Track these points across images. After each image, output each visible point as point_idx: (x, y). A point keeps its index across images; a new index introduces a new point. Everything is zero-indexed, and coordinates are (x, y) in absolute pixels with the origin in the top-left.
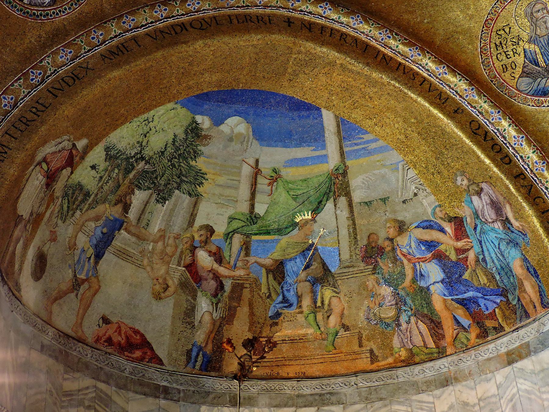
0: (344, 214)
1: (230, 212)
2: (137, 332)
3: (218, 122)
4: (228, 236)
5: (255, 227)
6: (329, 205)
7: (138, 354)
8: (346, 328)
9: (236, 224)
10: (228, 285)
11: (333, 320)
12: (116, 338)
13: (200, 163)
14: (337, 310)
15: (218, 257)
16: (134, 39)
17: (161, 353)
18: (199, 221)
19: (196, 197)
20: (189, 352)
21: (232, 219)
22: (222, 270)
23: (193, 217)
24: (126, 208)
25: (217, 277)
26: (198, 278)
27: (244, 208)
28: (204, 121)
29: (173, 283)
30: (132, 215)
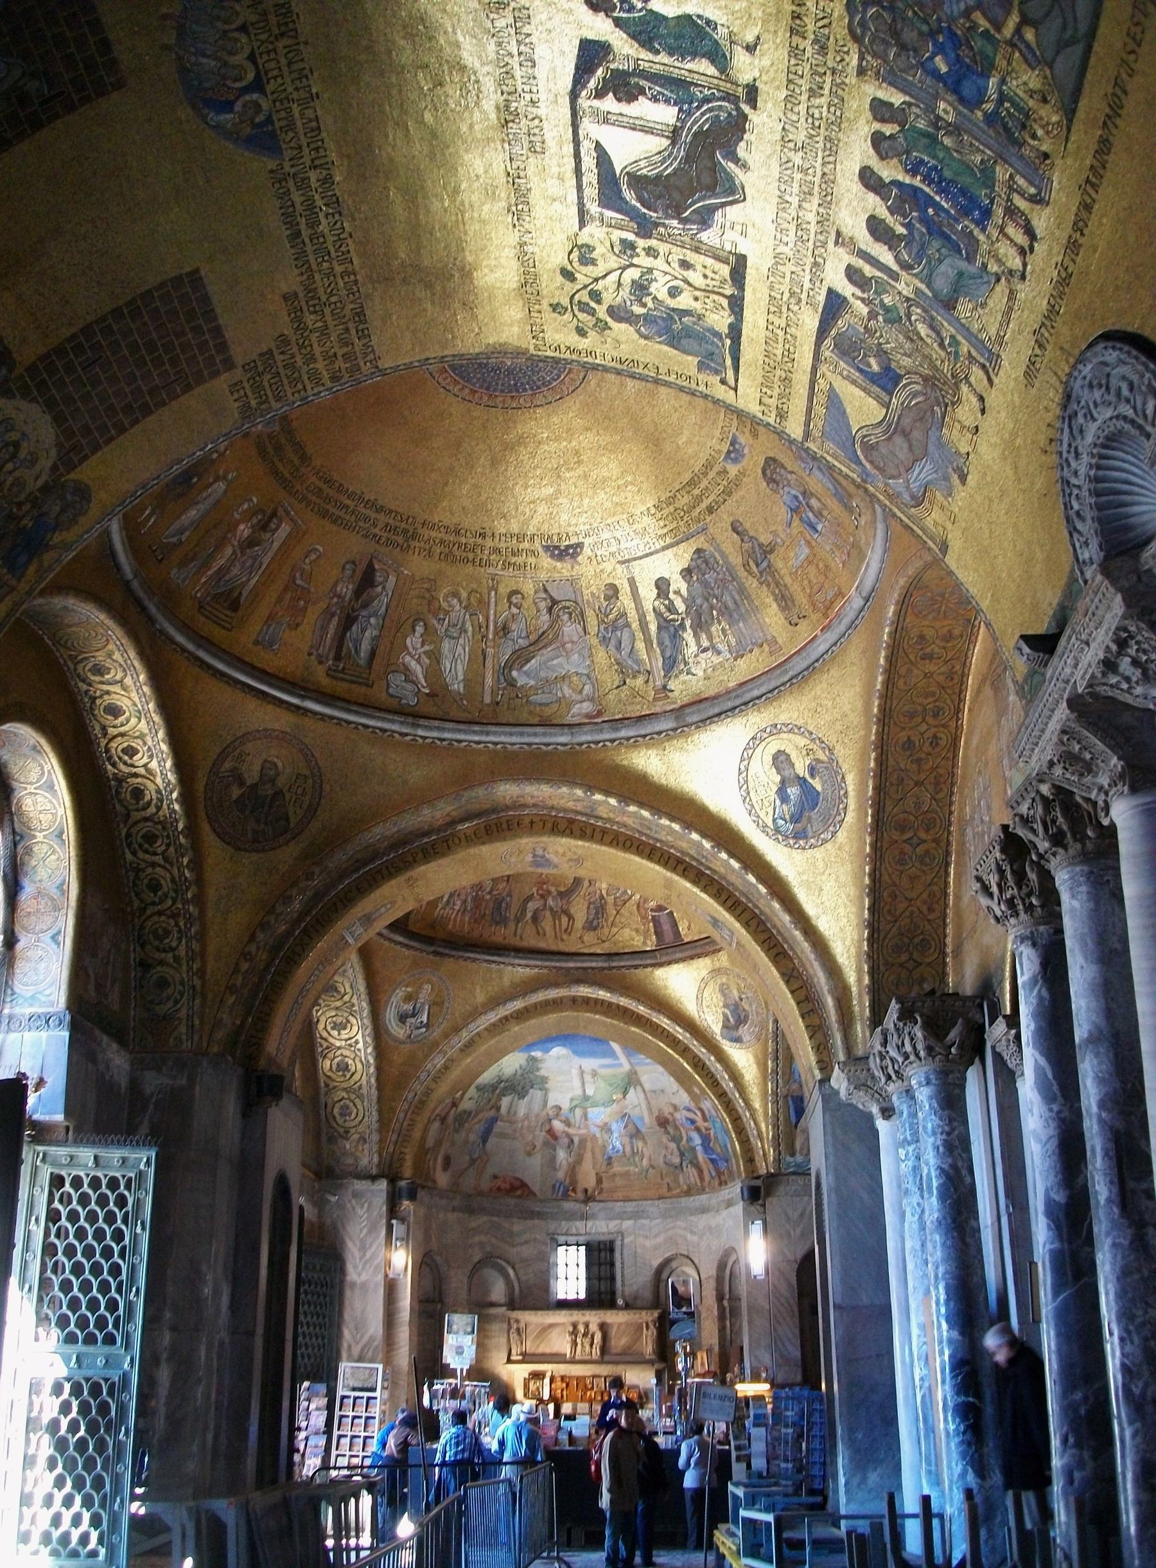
0: (642, 1096)
1: (570, 1096)
2: (517, 1179)
3: (548, 1051)
4: (572, 1109)
5: (588, 1104)
6: (632, 1090)
7: (519, 1192)
8: (653, 1167)
9: (575, 1103)
10: (576, 1140)
11: (645, 1162)
12: (503, 1186)
13: (543, 1073)
14: (646, 1154)
15: (568, 1123)
16: (478, 1034)
17: (535, 1189)
18: (551, 1103)
19: (546, 1091)
20: (554, 1186)
21: (572, 1100)
22: (571, 1131)
23: (545, 1102)
24: (498, 1109)
25: (568, 1135)
26: (555, 1138)
27: (579, 1092)
28: (537, 1054)
29: (539, 1144)
30: (503, 1110)
